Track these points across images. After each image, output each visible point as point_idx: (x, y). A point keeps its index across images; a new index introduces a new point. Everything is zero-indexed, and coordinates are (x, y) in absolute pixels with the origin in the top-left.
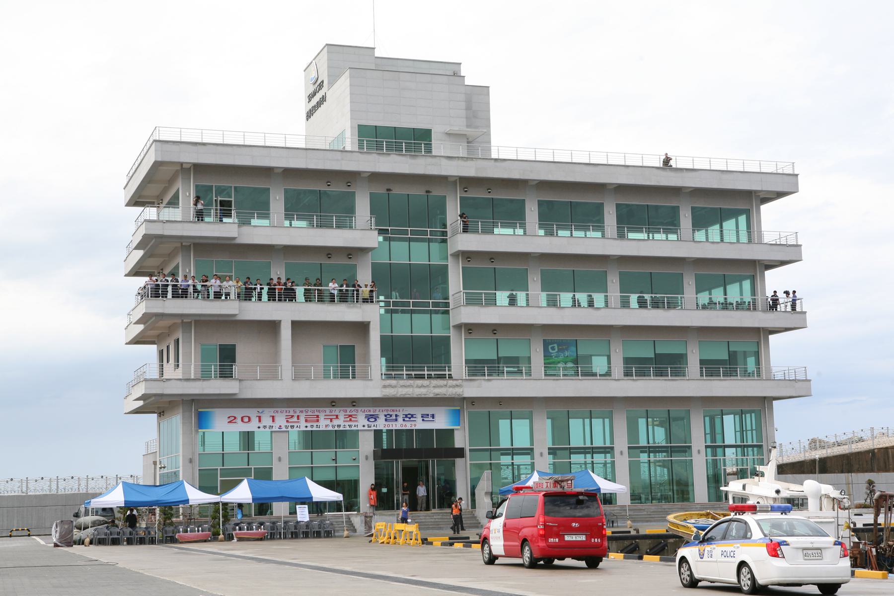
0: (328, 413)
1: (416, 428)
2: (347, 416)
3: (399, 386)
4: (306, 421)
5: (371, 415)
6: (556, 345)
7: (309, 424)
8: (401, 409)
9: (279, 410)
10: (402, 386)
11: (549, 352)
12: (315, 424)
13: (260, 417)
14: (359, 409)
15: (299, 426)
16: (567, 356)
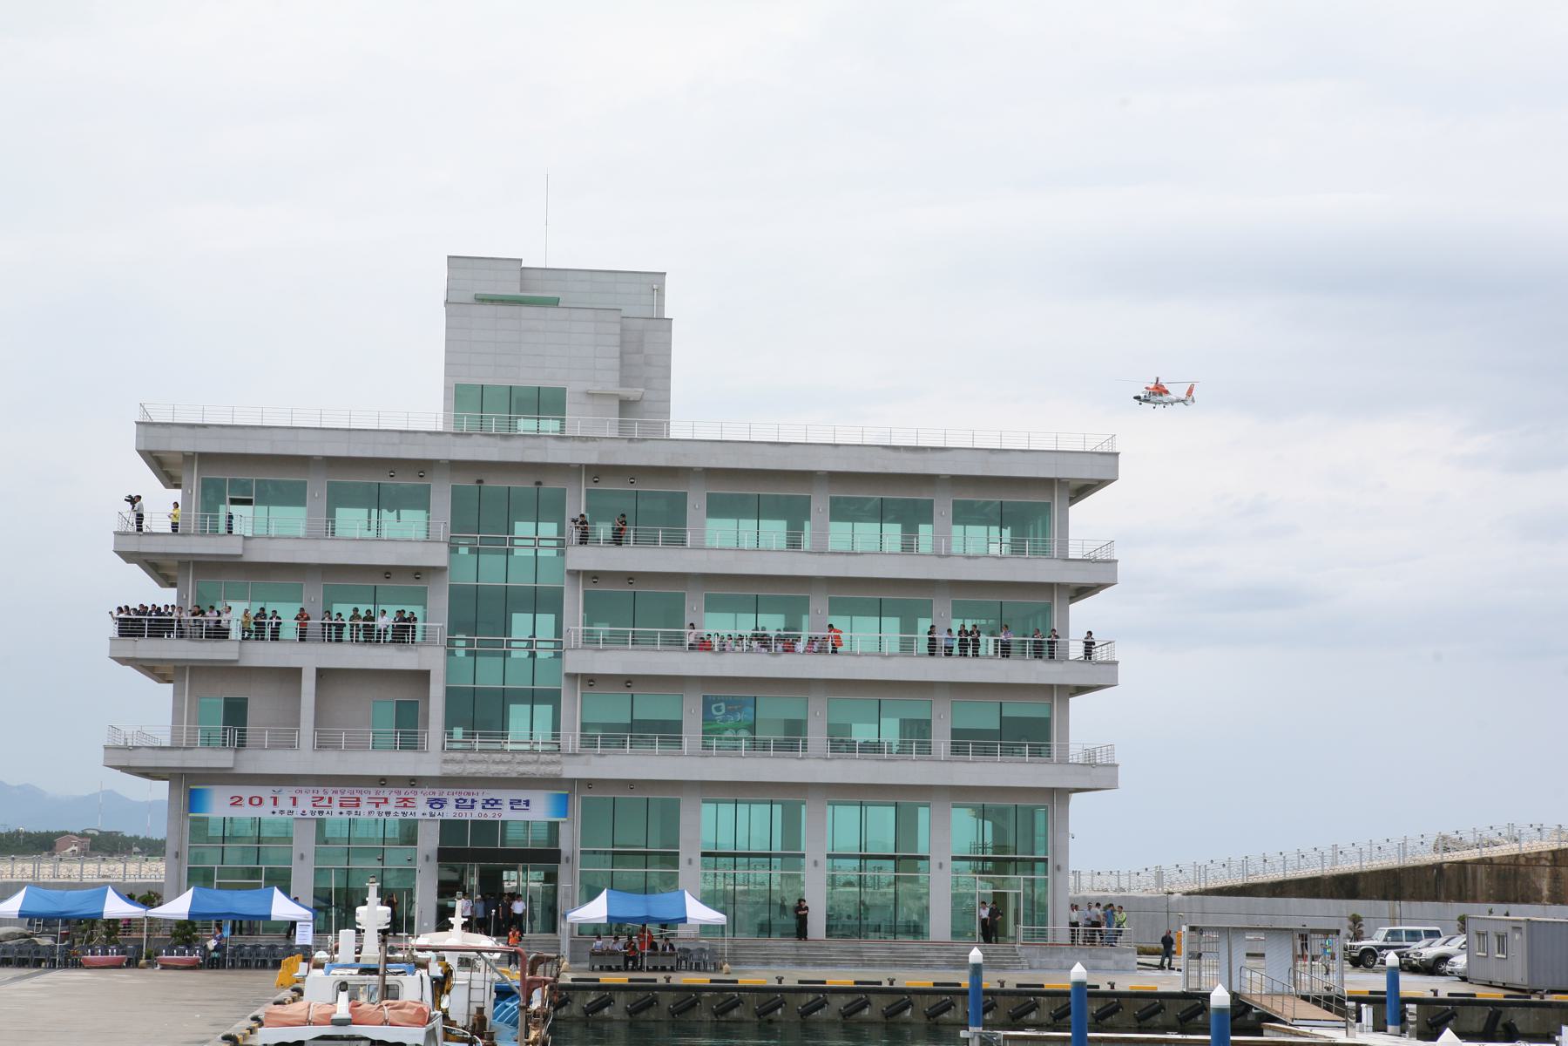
0: (373, 795)
4: (341, 805)
5: (436, 799)
6: (723, 705)
7: (344, 810)
8: (481, 791)
9: (303, 789)
10: (472, 762)
11: (712, 715)
12: (353, 810)
13: (275, 799)
14: (419, 790)
16: (740, 720)
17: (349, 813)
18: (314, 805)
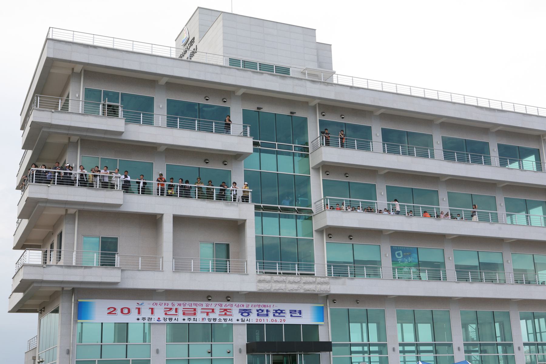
0: (204, 307)
1: (286, 323)
2: (223, 310)
3: (273, 281)
4: (184, 314)
5: (244, 310)
7: (186, 317)
8: (272, 304)
9: (158, 302)
12: (192, 317)
13: (139, 309)
14: (234, 304)
15: (177, 319)
17: (189, 319)
18: (166, 314)
